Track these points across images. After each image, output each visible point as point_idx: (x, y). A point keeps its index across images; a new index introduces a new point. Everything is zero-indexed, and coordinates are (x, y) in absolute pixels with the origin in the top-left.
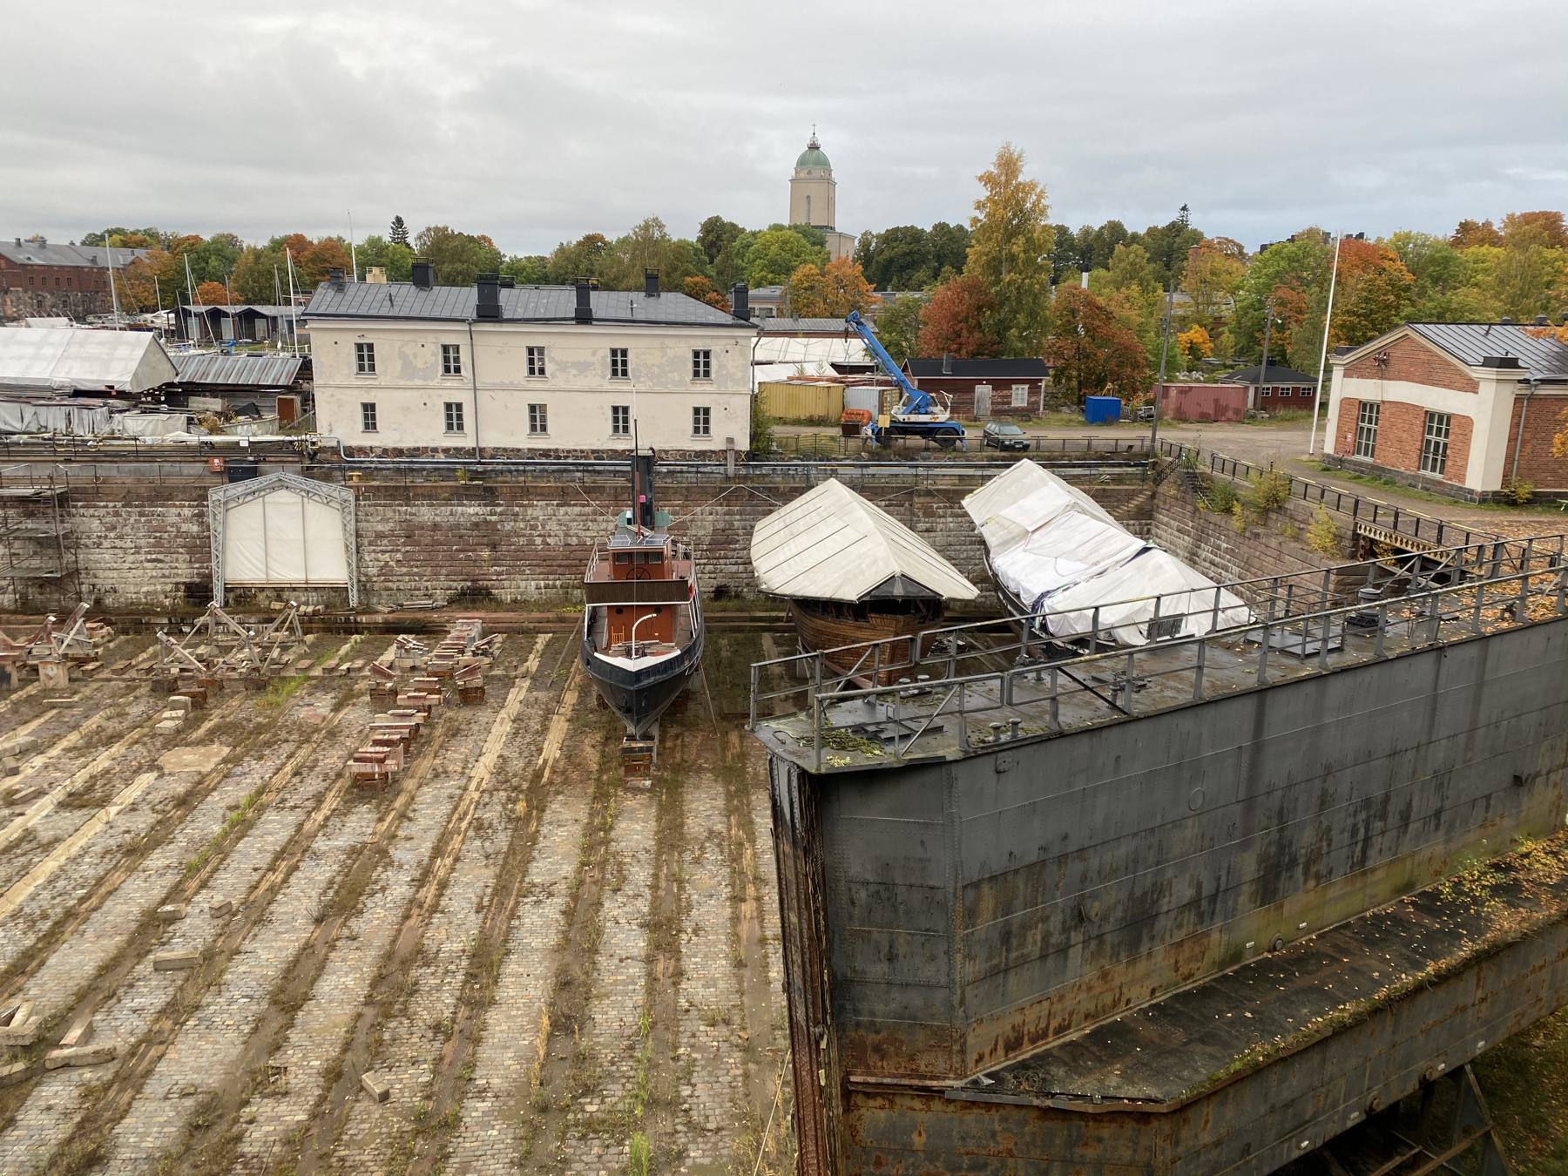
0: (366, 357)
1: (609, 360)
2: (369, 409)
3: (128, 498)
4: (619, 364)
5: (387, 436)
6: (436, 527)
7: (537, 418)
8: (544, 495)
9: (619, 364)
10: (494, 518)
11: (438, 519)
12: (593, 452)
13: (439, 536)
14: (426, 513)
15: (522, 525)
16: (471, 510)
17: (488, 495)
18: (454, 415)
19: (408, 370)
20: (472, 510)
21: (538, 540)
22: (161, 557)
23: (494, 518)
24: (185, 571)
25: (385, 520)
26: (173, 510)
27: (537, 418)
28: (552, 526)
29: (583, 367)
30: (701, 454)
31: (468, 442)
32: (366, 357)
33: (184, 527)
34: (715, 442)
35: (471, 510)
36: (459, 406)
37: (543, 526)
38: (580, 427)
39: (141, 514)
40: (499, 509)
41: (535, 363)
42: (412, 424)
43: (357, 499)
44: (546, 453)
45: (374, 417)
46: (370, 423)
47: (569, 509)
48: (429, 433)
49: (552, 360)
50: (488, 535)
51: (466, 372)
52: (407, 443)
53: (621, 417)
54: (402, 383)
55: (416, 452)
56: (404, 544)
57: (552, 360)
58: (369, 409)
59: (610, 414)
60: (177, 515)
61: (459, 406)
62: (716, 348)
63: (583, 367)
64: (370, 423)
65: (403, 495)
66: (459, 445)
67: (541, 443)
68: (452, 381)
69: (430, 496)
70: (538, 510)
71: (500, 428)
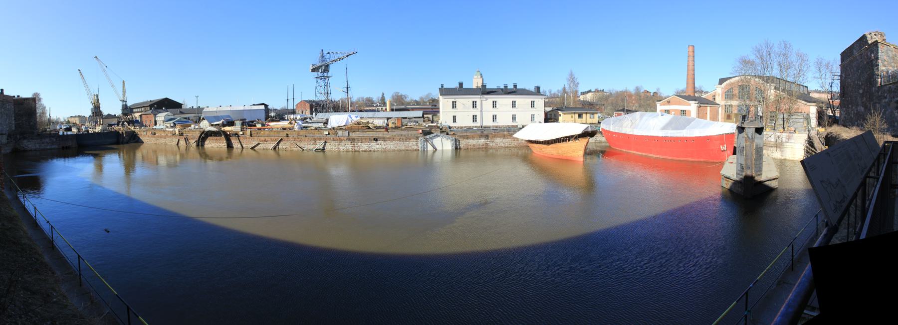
2: (454, 117)
4: (514, 104)
7: (494, 118)
9: (514, 104)
17: (487, 137)
18: (474, 118)
27: (494, 118)
31: (479, 125)
42: (464, 121)
46: (454, 121)
48: (470, 123)
53: (514, 118)
58: (454, 117)
64: (454, 121)
67: (495, 124)
68: (475, 110)
69: (473, 137)
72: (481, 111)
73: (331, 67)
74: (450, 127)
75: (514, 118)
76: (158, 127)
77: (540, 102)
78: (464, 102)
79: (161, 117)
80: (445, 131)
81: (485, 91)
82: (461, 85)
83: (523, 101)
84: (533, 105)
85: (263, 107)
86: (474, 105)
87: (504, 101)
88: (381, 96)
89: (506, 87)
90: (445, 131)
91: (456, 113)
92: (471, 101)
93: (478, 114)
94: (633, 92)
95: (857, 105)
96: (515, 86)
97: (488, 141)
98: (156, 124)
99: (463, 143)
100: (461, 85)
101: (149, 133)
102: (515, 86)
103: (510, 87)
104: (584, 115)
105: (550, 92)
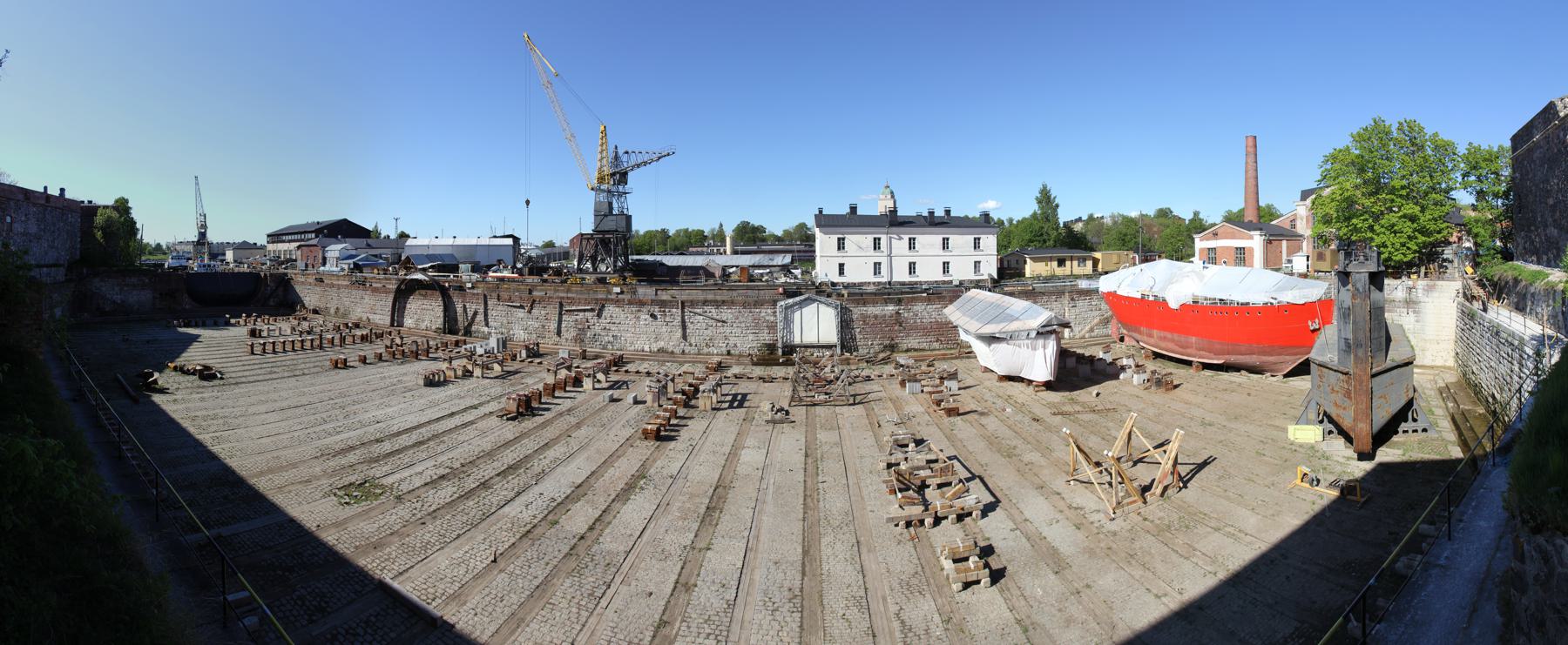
2: (841, 266)
3: (745, 305)
5: (851, 277)
6: (876, 317)
7: (912, 268)
9: (945, 244)
17: (899, 302)
20: (891, 308)
27: (912, 268)
31: (884, 280)
38: (929, 272)
42: (859, 272)
46: (841, 272)
48: (869, 277)
50: (898, 319)
52: (857, 281)
53: (946, 266)
55: (861, 284)
58: (841, 266)
60: (765, 313)
64: (841, 272)
70: (919, 307)
72: (890, 256)
73: (630, 175)
74: (833, 284)
75: (946, 266)
76: (327, 267)
77: (990, 242)
78: (859, 242)
79: (335, 250)
80: (823, 291)
81: (893, 221)
82: (853, 209)
83: (961, 241)
85: (510, 241)
86: (877, 244)
87: (929, 241)
88: (717, 227)
89: (931, 213)
90: (823, 291)
91: (848, 261)
93: (884, 261)
95: (1546, 226)
96: (948, 212)
98: (324, 264)
99: (857, 311)
100: (853, 209)
101: (311, 280)
102: (948, 212)
103: (939, 213)
104: (1068, 263)
105: (1011, 221)
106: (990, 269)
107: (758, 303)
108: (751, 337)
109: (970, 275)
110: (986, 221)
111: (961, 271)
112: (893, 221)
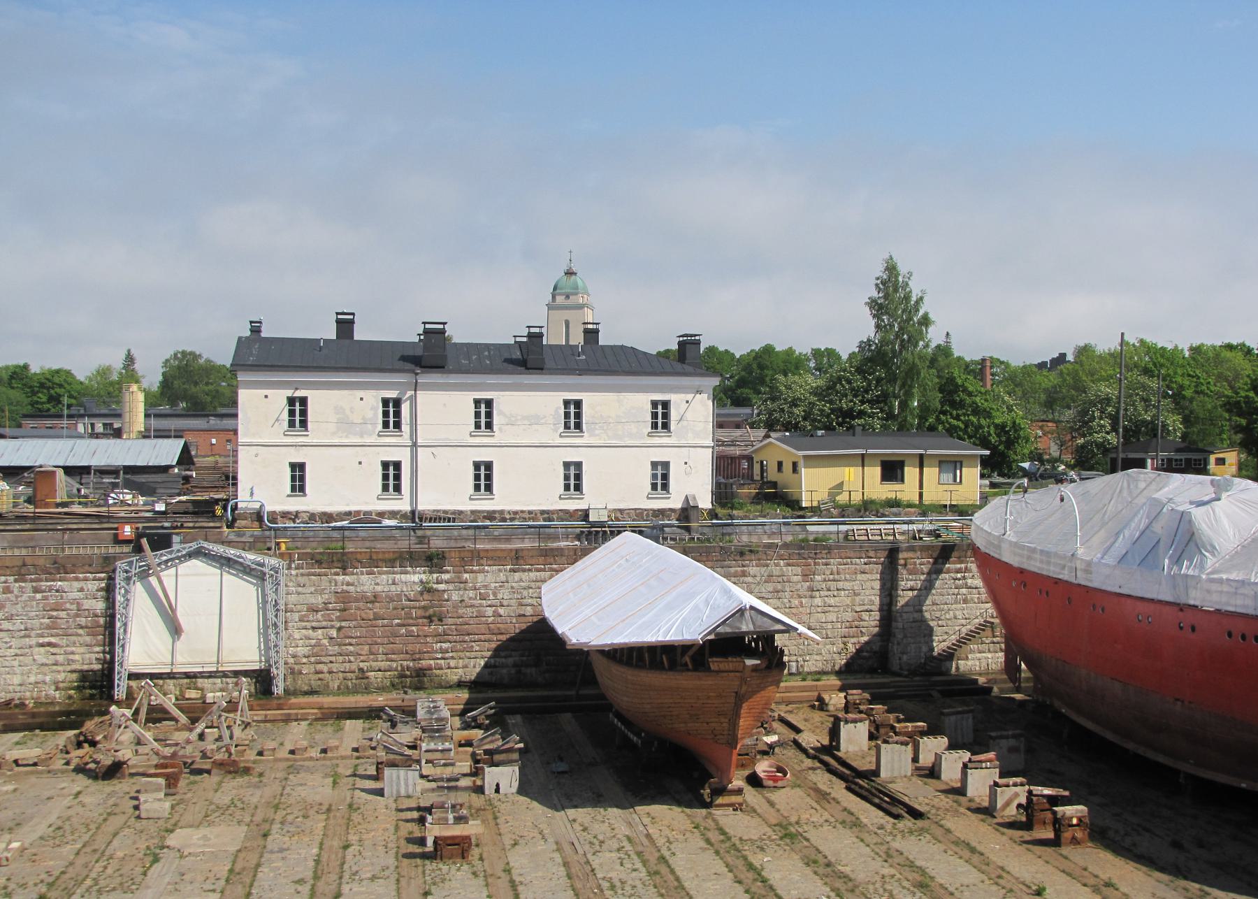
0: (298, 413)
1: (562, 410)
2: (298, 471)
4: (574, 417)
5: (321, 497)
6: (376, 598)
7: (484, 476)
8: (496, 558)
9: (574, 417)
10: (442, 587)
11: (379, 588)
12: (543, 512)
13: (377, 607)
14: (365, 582)
15: (471, 593)
16: (416, 578)
18: (391, 474)
19: (345, 424)
20: (415, 577)
21: (490, 611)
22: (53, 640)
23: (442, 587)
24: (87, 657)
25: (322, 592)
26: (76, 585)
27: (484, 476)
28: (504, 594)
29: (534, 420)
30: (661, 513)
31: (404, 505)
32: (298, 413)
33: (87, 604)
34: (674, 501)
35: (416, 578)
36: (397, 465)
37: (495, 594)
38: (528, 487)
39: (36, 590)
40: (445, 577)
41: (485, 416)
42: (345, 485)
43: (289, 568)
44: (490, 516)
45: (302, 478)
47: (525, 576)
48: (365, 496)
49: (501, 413)
51: (405, 427)
54: (336, 441)
56: (340, 619)
57: (501, 413)
58: (298, 471)
59: (561, 471)
60: (82, 592)
61: (397, 465)
62: (676, 399)
63: (534, 420)
65: (343, 562)
66: (396, 508)
67: (485, 505)
69: (373, 562)
70: (490, 577)
71: (442, 488)
77: (695, 409)
78: (346, 406)
81: (431, 355)
82: (345, 326)
83: (616, 407)
84: (661, 417)
86: (392, 414)
87: (529, 407)
91: (313, 456)
92: (279, 398)
94: (857, 350)
97: (442, 580)
100: (345, 326)
106: (694, 483)
107: (61, 568)
108: (41, 655)
109: (640, 497)
110: (687, 357)
111: (616, 485)
112: (431, 355)
